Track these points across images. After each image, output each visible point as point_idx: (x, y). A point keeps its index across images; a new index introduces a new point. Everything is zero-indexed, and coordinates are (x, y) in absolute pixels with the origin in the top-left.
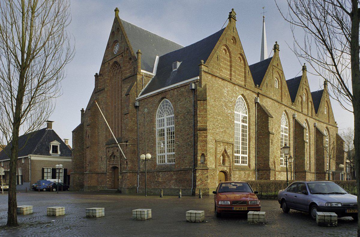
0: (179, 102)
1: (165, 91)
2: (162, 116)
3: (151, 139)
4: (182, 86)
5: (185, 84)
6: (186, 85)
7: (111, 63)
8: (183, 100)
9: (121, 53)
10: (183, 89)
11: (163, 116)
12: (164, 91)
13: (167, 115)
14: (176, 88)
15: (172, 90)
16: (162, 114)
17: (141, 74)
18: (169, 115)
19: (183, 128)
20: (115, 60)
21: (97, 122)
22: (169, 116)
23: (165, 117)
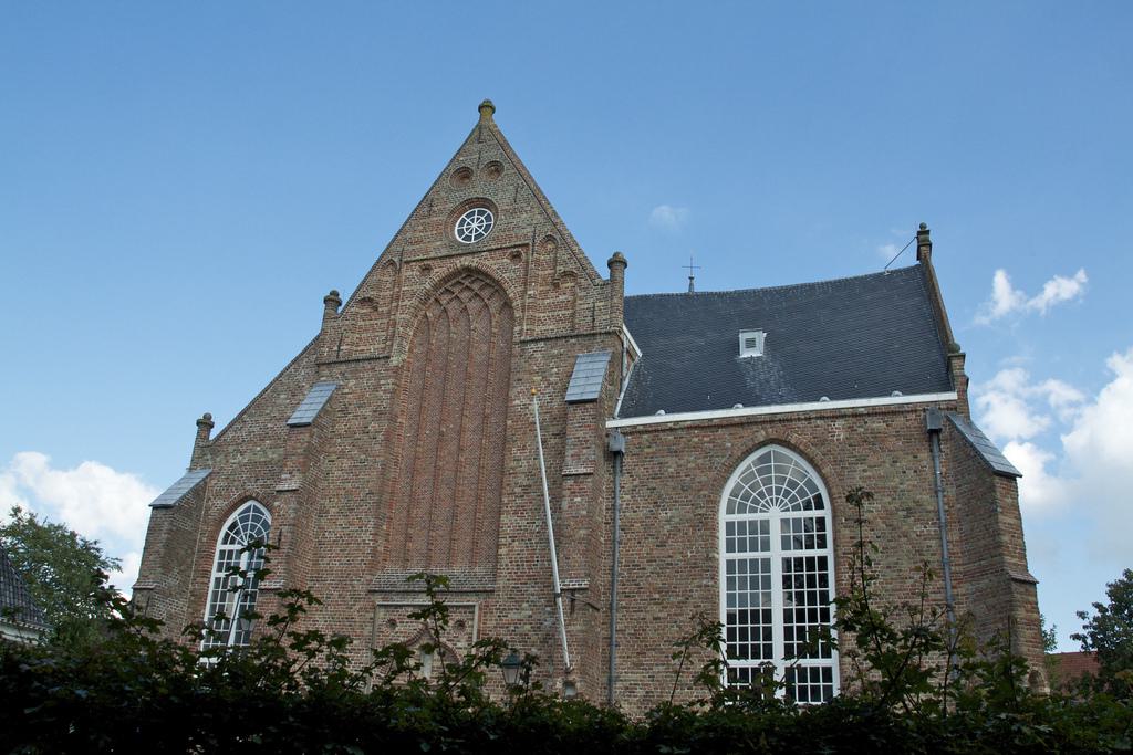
0: (860, 467)
1: (786, 419)
2: (754, 510)
3: (696, 594)
4: (874, 412)
5: (892, 408)
6: (894, 413)
7: (440, 271)
8: (884, 462)
9: (515, 246)
10: (878, 424)
11: (761, 511)
12: (779, 417)
13: (788, 510)
14: (844, 416)
15: (822, 418)
16: (756, 502)
17: (621, 336)
18: (797, 508)
19: (888, 567)
20: (466, 261)
21: (320, 486)
22: (792, 515)
23: (775, 516)
